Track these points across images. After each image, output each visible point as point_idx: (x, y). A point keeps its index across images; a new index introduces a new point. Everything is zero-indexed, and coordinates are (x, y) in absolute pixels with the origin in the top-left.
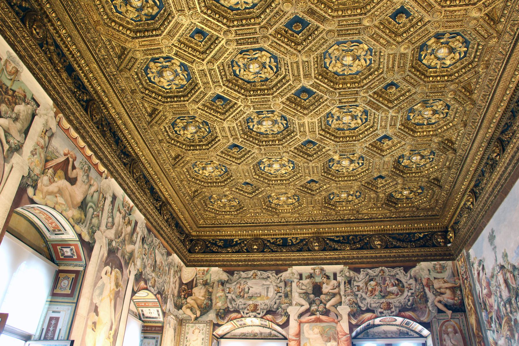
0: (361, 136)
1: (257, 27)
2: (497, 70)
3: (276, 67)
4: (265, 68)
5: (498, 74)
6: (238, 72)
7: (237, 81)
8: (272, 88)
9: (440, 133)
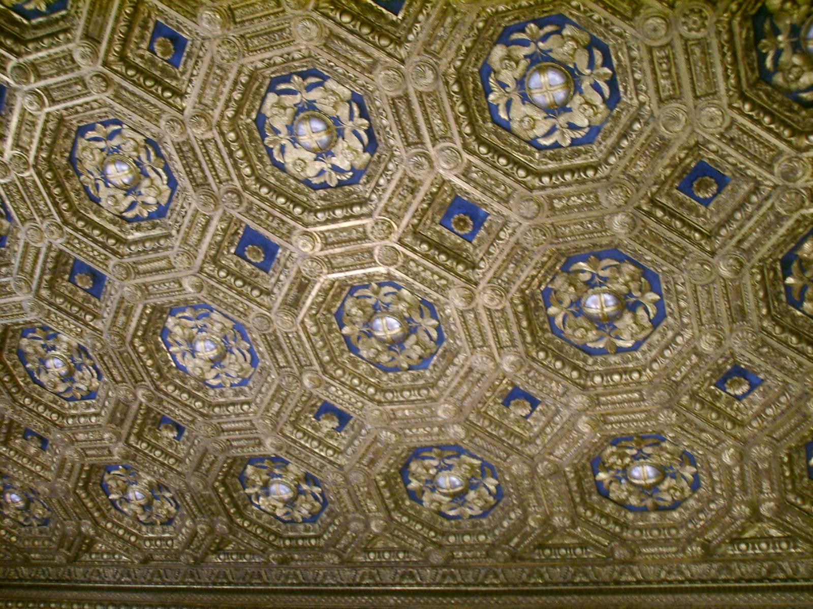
0: (27, 401)
1: (237, 184)
2: (282, 579)
3: (137, 218)
4: (126, 195)
5: (276, 585)
6: (91, 134)
7: (67, 136)
8: (80, 218)
9: (105, 528)
